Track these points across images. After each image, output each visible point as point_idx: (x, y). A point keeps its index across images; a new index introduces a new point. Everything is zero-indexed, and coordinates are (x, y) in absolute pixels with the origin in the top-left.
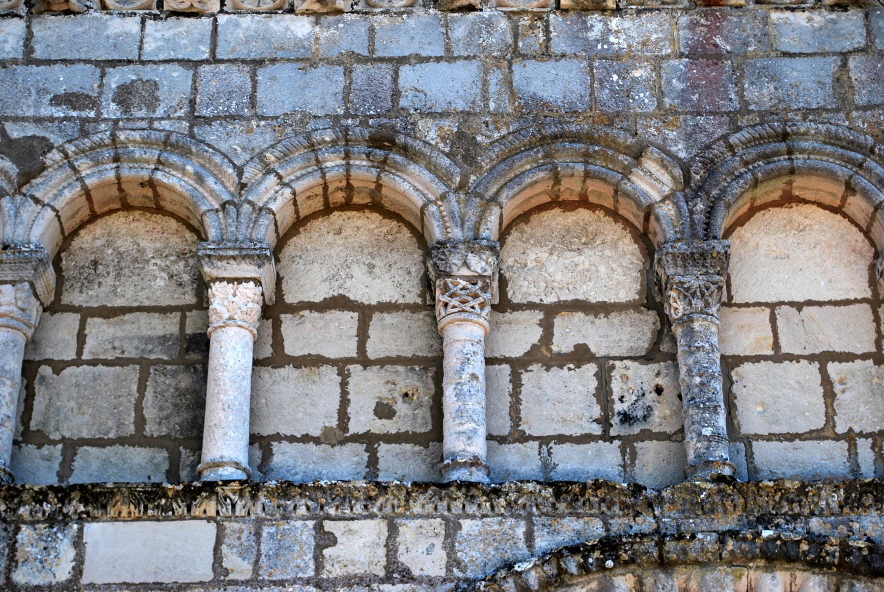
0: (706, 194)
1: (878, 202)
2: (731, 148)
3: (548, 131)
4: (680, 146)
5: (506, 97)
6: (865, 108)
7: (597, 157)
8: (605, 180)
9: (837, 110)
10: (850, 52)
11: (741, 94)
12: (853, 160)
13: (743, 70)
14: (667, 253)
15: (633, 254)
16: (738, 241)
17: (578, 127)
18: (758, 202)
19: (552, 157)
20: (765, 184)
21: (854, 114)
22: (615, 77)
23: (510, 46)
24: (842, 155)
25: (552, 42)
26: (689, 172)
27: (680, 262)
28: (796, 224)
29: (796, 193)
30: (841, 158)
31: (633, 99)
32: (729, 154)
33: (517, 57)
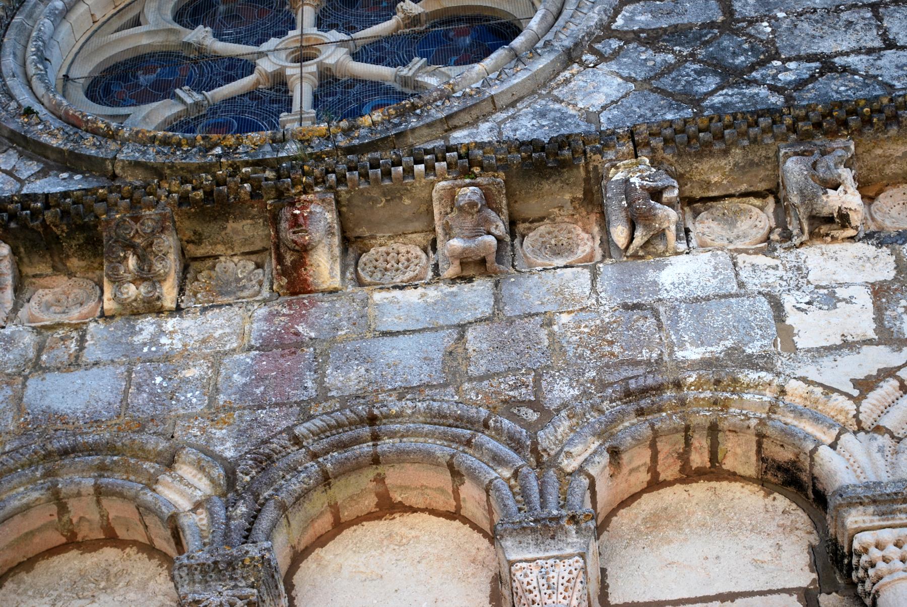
0: (253, 494)
1: (487, 481)
2: (297, 441)
3: (56, 445)
4: (228, 445)
5: (11, 414)
6: (481, 379)
7: (116, 469)
8: (121, 495)
9: (445, 385)
10: (471, 323)
11: (320, 382)
12: (458, 437)
13: (328, 355)
14: (181, 566)
15: (165, 595)
16: (314, 566)
17: (97, 437)
18: (345, 515)
19: (57, 475)
20: (343, 481)
21: (466, 386)
22: (159, 380)
23: (30, 360)
24: (445, 433)
25: (85, 350)
26: (234, 473)
27: (198, 577)
28: (398, 538)
29: (397, 497)
30: (444, 437)
31: (178, 400)
32: (295, 448)
33: (37, 371)
